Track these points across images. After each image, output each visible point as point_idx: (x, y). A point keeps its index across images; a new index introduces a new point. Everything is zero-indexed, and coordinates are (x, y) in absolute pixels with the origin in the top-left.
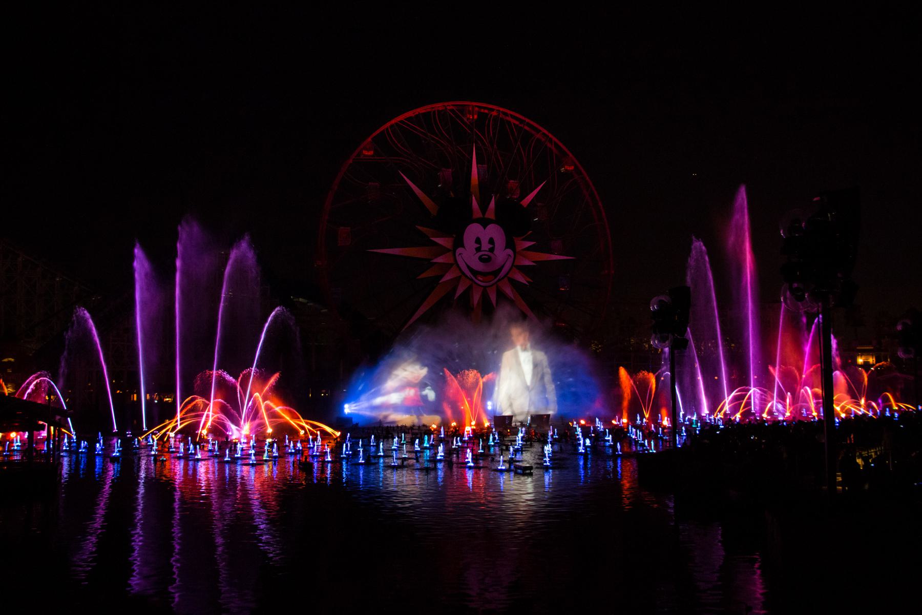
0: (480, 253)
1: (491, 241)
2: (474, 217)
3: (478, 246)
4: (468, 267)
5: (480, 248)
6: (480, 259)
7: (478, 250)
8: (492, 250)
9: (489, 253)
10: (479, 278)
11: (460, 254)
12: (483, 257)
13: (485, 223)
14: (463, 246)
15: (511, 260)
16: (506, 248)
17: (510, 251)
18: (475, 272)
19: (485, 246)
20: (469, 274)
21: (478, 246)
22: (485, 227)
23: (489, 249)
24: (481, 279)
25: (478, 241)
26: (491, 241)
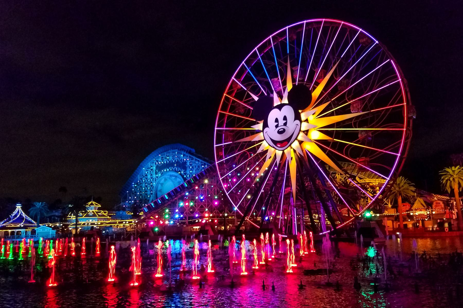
0: (278, 128)
1: (285, 118)
2: (275, 104)
3: (277, 123)
4: (272, 140)
5: (278, 124)
6: (279, 132)
7: (277, 126)
8: (285, 124)
10: (279, 146)
12: (280, 130)
13: (280, 107)
14: (268, 127)
15: (298, 127)
16: (294, 120)
17: (297, 122)
18: (275, 142)
19: (281, 122)
20: (272, 144)
21: (277, 123)
22: (280, 110)
25: (277, 120)
26: (285, 118)
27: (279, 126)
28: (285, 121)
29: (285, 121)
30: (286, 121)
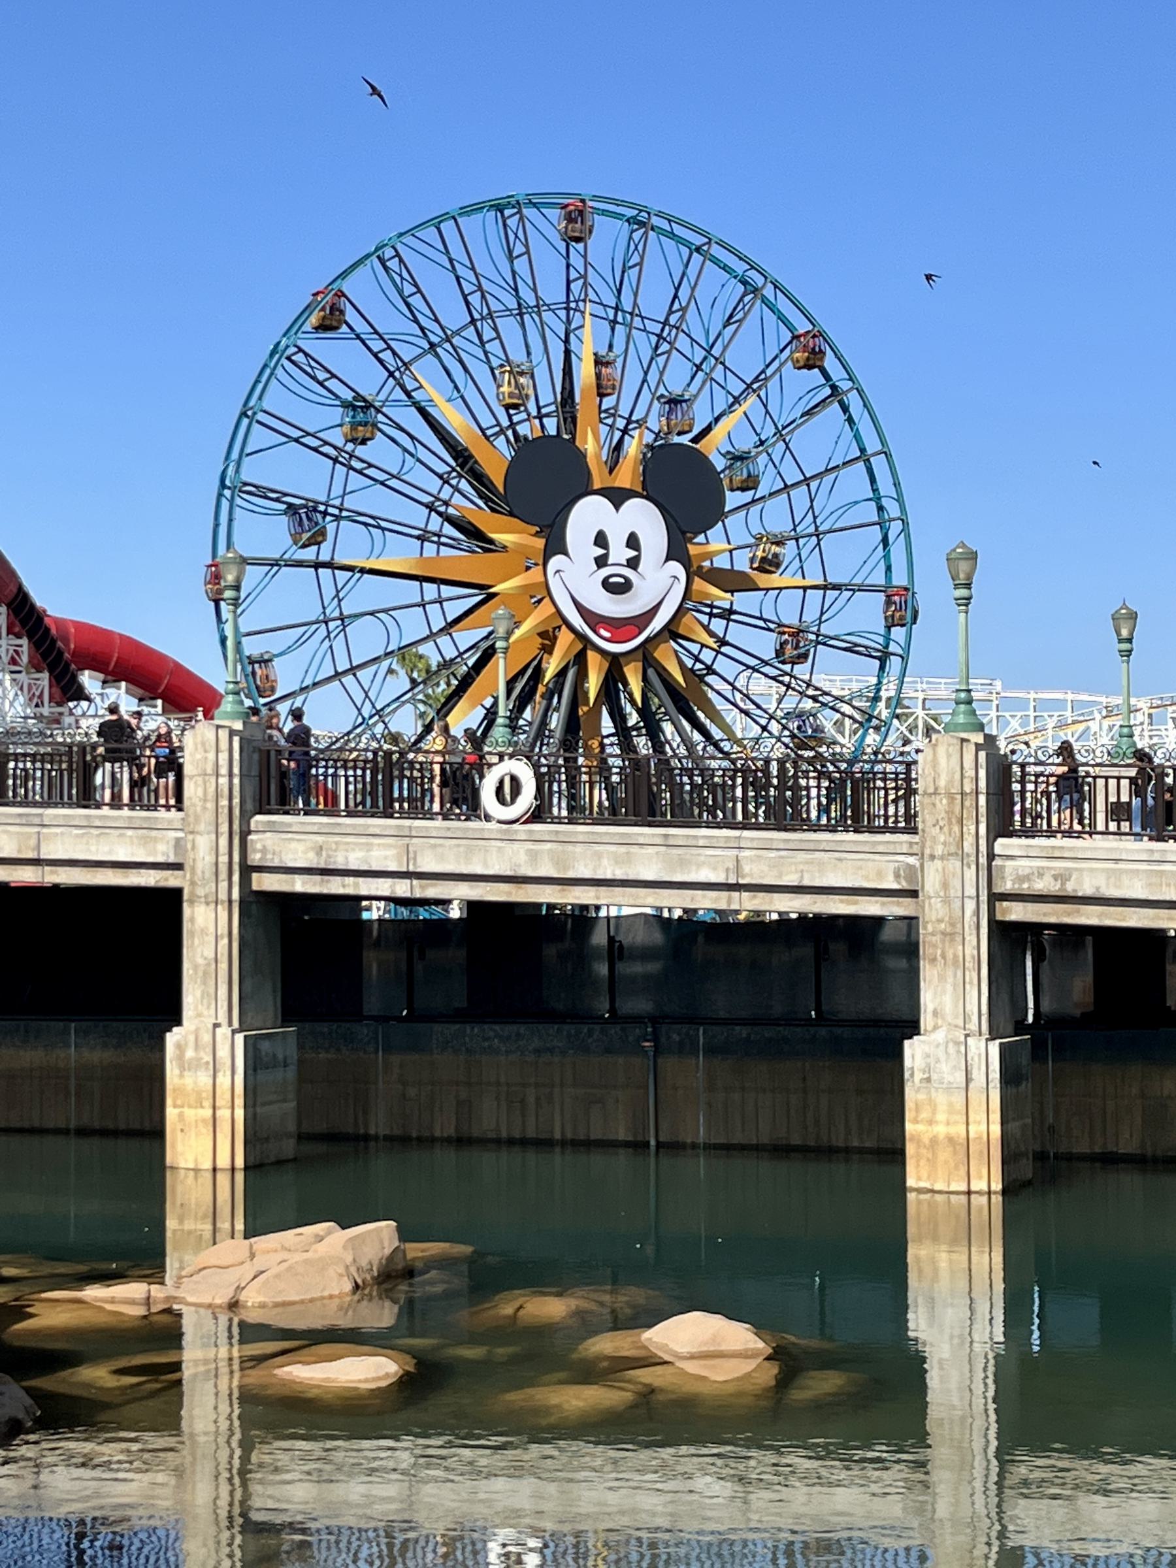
0: (605, 572)
1: (633, 542)
3: (601, 552)
6: (606, 584)
7: (601, 562)
8: (633, 563)
9: (627, 572)
11: (558, 571)
13: (617, 497)
14: (566, 554)
16: (667, 559)
17: (676, 568)
18: (593, 619)
19: (619, 553)
21: (601, 552)
22: (617, 507)
23: (628, 560)
24: (607, 634)
25: (601, 540)
26: (633, 542)
27: (610, 562)
28: (633, 553)
29: (633, 553)
30: (634, 553)
